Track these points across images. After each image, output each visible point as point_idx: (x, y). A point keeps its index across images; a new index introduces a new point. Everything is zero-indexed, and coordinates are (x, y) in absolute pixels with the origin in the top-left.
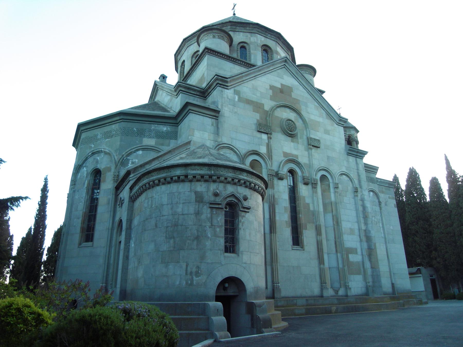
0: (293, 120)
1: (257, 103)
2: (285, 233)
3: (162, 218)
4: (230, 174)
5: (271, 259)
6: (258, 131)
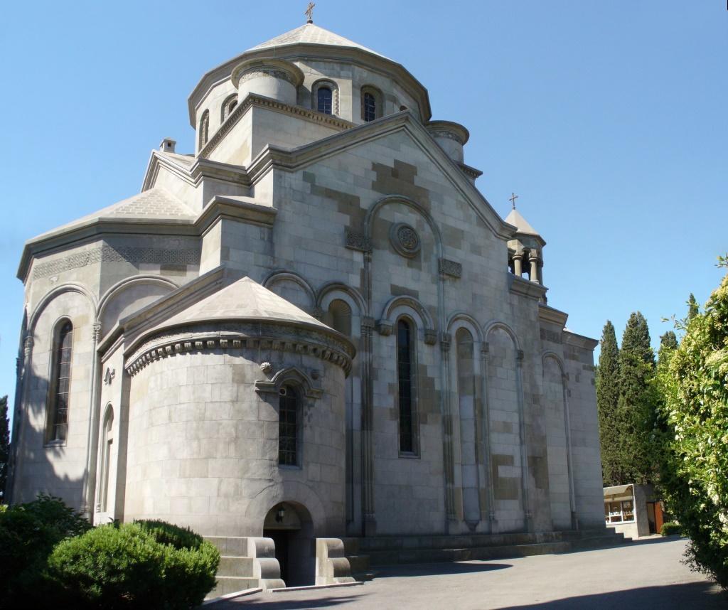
0: (414, 226)
1: (346, 195)
2: (389, 430)
3: (178, 407)
4: (289, 338)
5: (359, 472)
6: (346, 247)
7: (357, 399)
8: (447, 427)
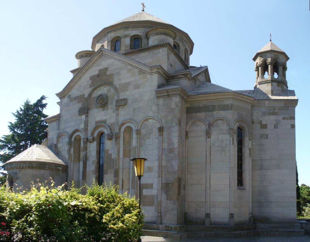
6: (80, 115)
7: (81, 169)
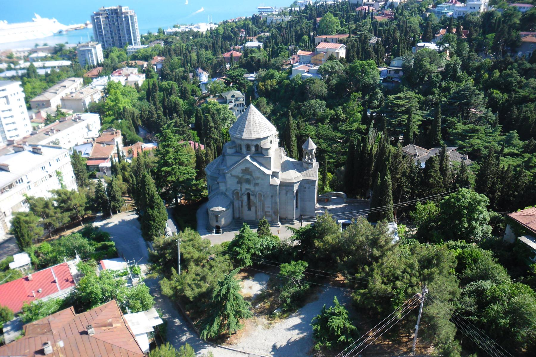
2: (245, 208)
8: (256, 207)
